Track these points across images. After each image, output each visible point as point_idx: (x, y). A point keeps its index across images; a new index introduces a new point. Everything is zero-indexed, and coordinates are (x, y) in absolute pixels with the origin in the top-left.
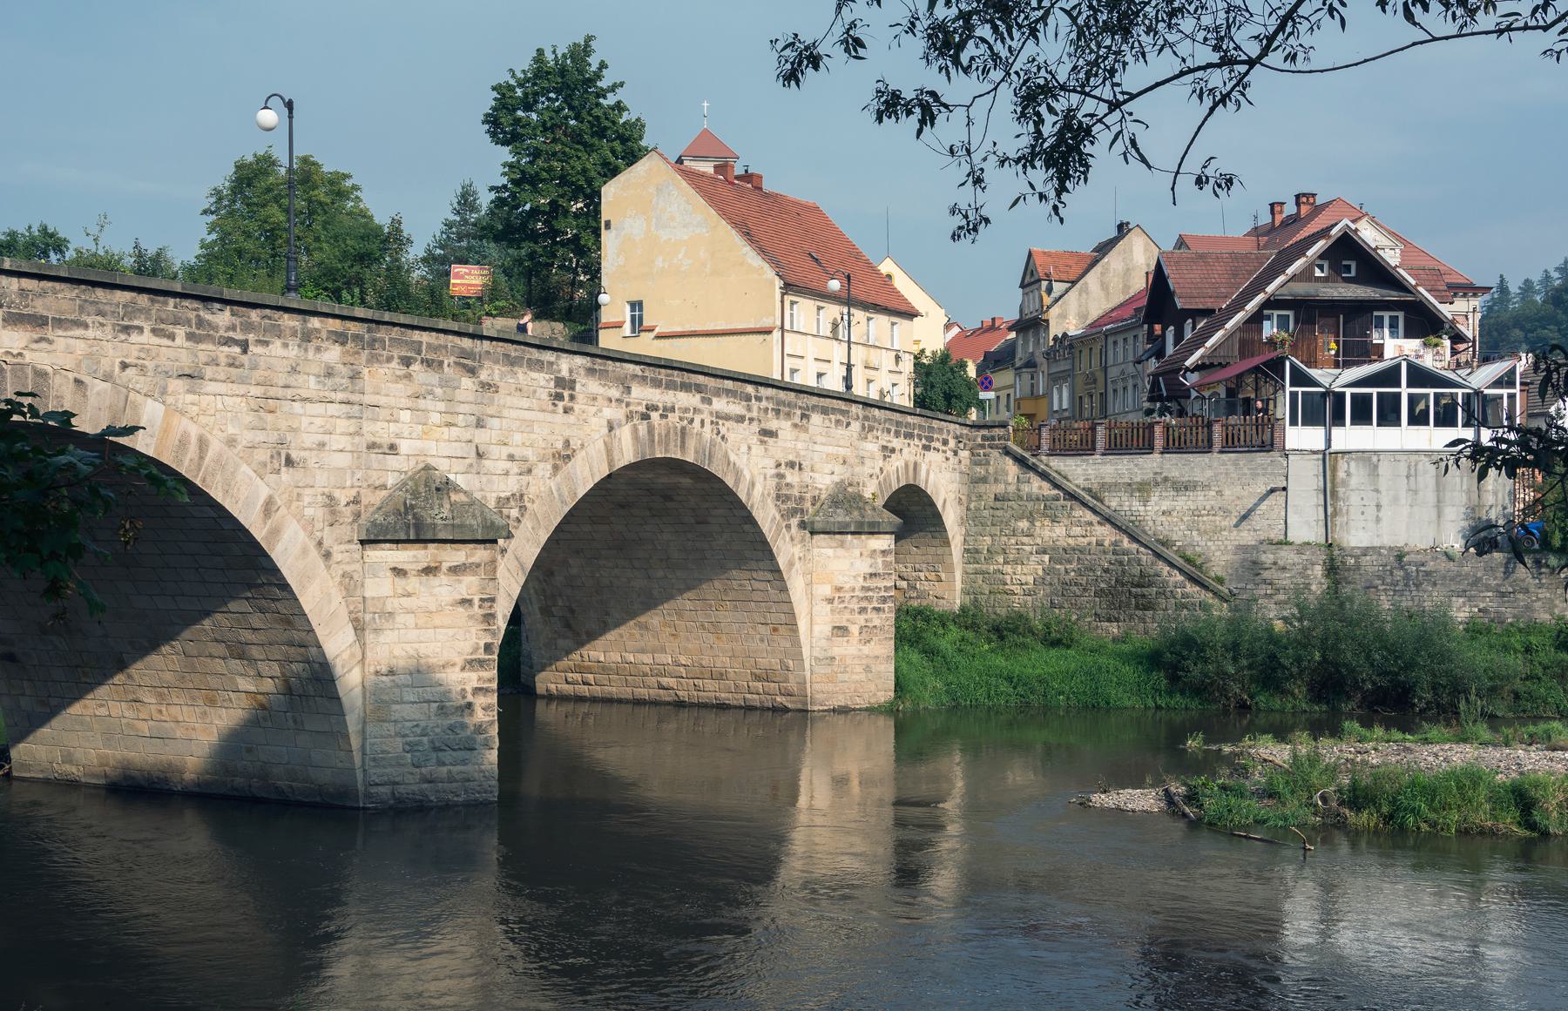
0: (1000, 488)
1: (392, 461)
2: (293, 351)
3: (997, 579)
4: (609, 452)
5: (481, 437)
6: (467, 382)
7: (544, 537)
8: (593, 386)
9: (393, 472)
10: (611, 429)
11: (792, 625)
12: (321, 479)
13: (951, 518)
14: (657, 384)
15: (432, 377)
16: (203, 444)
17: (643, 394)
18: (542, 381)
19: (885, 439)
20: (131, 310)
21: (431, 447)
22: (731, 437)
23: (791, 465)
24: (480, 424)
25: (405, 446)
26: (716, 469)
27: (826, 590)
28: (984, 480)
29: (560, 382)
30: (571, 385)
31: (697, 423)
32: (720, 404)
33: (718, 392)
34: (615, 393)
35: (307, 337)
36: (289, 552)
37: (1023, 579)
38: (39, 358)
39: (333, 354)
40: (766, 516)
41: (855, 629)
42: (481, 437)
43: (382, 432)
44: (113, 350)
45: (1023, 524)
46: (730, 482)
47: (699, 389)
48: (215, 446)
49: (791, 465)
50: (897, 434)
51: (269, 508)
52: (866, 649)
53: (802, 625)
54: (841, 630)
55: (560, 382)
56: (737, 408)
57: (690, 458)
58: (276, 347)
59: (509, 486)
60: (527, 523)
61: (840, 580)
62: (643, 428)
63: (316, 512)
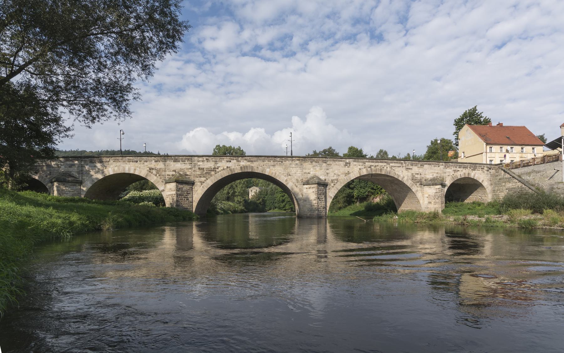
0: (500, 177)
1: (309, 175)
2: (290, 162)
3: (498, 196)
4: (360, 173)
5: (327, 171)
6: (324, 164)
7: (343, 185)
8: (355, 163)
9: (309, 176)
10: (360, 169)
11: (418, 201)
12: (295, 177)
13: (485, 184)
14: (372, 162)
15: (317, 164)
16: (275, 173)
17: (368, 164)
18: (342, 163)
19: (455, 169)
20: (264, 159)
21: (317, 173)
22: (396, 170)
23: (417, 174)
24: (327, 169)
25: (311, 173)
26: (392, 175)
27: (427, 195)
28: (497, 176)
29: (346, 163)
30: (350, 163)
31: (385, 168)
32: (391, 164)
33: (392, 163)
34: (361, 164)
35: (293, 160)
36: (290, 185)
37: (502, 195)
38: (252, 165)
39: (297, 162)
40: (409, 183)
41: (433, 202)
42: (327, 171)
43: (307, 171)
44: (261, 163)
45: (504, 184)
46: (396, 177)
47: (385, 162)
48: (277, 173)
49: (417, 174)
50: (459, 168)
51: (286, 180)
52: (435, 206)
53: (421, 202)
54: (430, 203)
55: (346, 163)
56: (398, 165)
57: (383, 173)
58: (287, 162)
59: (335, 178)
60: (339, 183)
61: (430, 194)
62: (369, 169)
63: (295, 181)
